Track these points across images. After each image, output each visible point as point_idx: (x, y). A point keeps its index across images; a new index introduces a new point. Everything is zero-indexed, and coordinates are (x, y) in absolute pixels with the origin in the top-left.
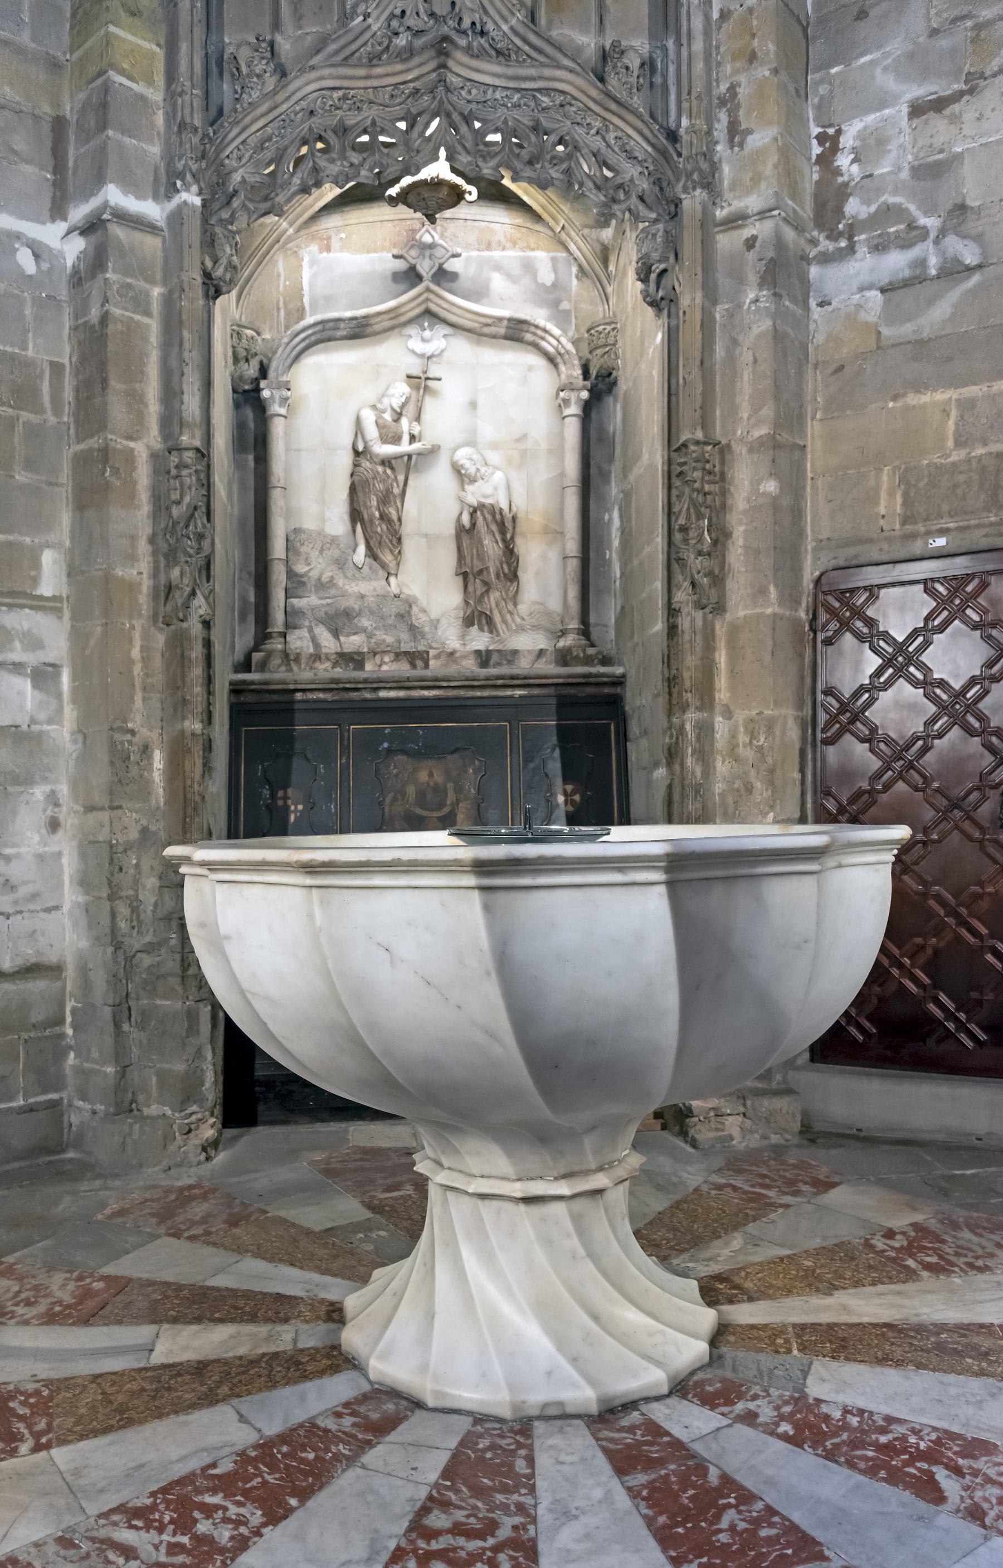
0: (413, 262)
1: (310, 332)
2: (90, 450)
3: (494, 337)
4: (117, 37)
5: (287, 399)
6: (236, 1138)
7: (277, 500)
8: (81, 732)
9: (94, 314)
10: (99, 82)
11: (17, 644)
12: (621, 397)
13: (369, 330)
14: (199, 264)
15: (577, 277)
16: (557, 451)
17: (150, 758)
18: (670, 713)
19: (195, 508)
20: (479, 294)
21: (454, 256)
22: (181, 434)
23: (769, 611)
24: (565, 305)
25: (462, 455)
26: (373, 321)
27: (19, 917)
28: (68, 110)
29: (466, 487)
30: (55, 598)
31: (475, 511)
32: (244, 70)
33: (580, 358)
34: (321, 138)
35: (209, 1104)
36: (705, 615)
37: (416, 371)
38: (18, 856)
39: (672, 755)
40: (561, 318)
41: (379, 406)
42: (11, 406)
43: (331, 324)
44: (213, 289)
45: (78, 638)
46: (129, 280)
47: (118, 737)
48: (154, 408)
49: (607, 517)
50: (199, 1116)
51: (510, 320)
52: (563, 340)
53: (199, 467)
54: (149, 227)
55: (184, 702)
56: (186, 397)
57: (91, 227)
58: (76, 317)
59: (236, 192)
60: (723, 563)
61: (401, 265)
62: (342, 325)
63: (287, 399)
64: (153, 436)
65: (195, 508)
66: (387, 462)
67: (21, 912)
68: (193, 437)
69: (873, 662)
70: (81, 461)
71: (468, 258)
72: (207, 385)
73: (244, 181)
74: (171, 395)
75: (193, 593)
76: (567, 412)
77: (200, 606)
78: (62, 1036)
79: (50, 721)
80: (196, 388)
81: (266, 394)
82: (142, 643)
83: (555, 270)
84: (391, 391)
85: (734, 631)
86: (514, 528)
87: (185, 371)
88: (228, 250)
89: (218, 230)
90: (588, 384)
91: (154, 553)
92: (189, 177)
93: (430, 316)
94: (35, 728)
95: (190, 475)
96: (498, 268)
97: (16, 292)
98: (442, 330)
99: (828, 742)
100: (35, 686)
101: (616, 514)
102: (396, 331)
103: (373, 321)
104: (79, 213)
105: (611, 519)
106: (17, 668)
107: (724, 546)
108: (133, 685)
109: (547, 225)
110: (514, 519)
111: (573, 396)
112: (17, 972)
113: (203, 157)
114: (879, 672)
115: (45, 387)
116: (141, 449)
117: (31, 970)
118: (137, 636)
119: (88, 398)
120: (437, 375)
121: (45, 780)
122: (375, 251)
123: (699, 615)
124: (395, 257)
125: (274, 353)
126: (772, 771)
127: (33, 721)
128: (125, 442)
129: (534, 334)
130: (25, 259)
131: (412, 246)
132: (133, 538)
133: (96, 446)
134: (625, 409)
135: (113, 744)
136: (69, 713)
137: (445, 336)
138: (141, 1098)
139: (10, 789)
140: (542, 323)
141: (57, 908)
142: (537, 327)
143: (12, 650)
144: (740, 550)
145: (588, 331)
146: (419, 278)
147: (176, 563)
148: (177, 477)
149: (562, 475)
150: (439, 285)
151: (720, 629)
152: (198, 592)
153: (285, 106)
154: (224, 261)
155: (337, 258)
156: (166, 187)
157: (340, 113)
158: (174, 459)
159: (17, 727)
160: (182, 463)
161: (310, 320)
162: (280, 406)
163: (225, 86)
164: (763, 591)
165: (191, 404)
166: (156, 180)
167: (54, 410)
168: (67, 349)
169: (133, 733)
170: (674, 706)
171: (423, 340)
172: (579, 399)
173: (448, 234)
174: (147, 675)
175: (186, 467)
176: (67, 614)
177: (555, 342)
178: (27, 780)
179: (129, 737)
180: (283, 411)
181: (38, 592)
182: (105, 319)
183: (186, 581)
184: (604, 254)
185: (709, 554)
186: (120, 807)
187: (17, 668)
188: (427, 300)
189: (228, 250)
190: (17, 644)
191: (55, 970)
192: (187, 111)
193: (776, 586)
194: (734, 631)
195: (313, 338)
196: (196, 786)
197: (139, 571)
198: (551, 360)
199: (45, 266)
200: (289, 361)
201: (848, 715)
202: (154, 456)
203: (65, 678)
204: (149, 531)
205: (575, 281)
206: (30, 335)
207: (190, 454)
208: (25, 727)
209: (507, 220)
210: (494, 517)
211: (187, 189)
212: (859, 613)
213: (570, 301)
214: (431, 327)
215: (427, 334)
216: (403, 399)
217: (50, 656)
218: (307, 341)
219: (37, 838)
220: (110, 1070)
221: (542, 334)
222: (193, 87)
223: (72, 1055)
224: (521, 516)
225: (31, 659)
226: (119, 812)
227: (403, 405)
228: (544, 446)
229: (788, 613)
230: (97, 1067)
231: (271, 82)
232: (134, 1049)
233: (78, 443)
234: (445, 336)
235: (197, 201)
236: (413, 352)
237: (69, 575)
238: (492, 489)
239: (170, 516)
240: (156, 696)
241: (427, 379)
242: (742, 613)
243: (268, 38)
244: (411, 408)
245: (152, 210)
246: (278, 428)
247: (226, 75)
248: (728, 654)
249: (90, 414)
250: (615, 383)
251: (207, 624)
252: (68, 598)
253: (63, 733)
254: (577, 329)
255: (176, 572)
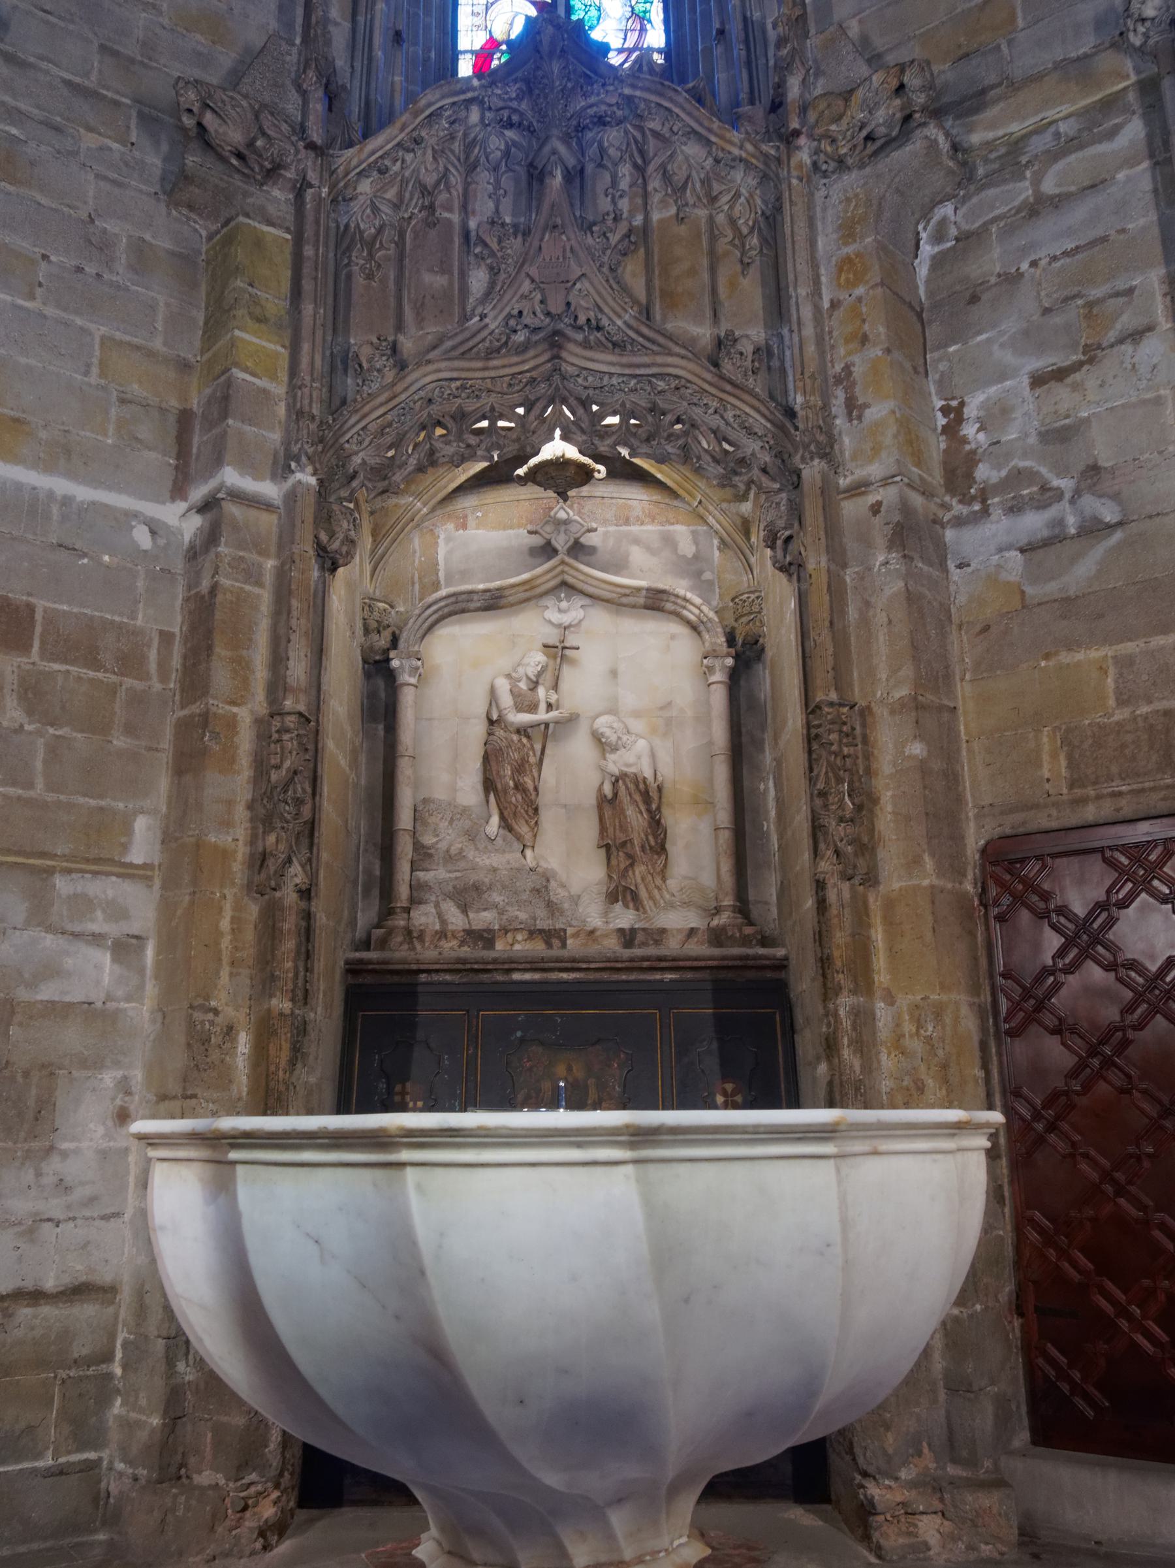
0: (548, 537)
1: (442, 604)
2: (192, 716)
3: (634, 606)
4: (242, 340)
5: (417, 668)
6: (311, 1521)
7: (405, 769)
8: (162, 1012)
9: (205, 585)
10: (223, 378)
11: (99, 914)
12: (768, 663)
13: (503, 601)
14: (312, 537)
15: (719, 549)
16: (703, 719)
17: (234, 1040)
18: (825, 998)
19: (295, 773)
20: (618, 565)
21: (590, 531)
22: (284, 699)
23: (926, 882)
24: (707, 576)
25: (603, 723)
26: (507, 593)
27: (71, 1224)
28: (195, 403)
29: (608, 755)
30: (145, 866)
31: (617, 781)
32: (365, 365)
33: (724, 627)
34: (439, 424)
35: (273, 1472)
36: (852, 886)
37: (553, 640)
38: (77, 1151)
39: (830, 1047)
40: (704, 588)
41: (514, 675)
42: (114, 673)
43: (464, 596)
44: (330, 563)
45: (166, 908)
46: (241, 554)
47: (198, 1015)
48: (260, 674)
49: (762, 787)
50: (259, 1488)
51: (648, 590)
52: (705, 608)
53: (302, 732)
54: (268, 507)
55: (273, 978)
56: (291, 664)
57: (207, 506)
58: (189, 590)
59: (355, 473)
60: (872, 830)
61: (537, 541)
62: (476, 597)
63: (417, 668)
64: (258, 702)
65: (295, 773)
66: (523, 731)
67: (74, 1219)
68: (297, 702)
69: (1053, 941)
70: (184, 728)
71: (606, 533)
72: (319, 651)
73: (364, 462)
74: (278, 661)
75: (289, 861)
76: (713, 679)
77: (297, 874)
78: (109, 1376)
79: (129, 999)
80: (302, 654)
81: (395, 663)
82: (232, 914)
83: (696, 543)
84: (525, 661)
85: (889, 905)
86: (660, 798)
87: (292, 637)
88: (345, 525)
89: (335, 507)
90: (732, 651)
91: (252, 820)
92: (304, 459)
93: (566, 587)
94: (111, 1005)
95: (292, 739)
96: (636, 541)
97: (129, 565)
98: (579, 601)
99: (1013, 1033)
100: (114, 960)
101: (771, 784)
102: (533, 602)
103: (507, 593)
104: (198, 493)
105: (766, 789)
106: (97, 939)
107: (871, 811)
108: (220, 960)
109: (683, 500)
110: (660, 789)
111: (717, 663)
112: (62, 1293)
113: (321, 441)
114: (1061, 953)
115: (153, 655)
116: (244, 715)
117: (79, 1291)
118: (228, 907)
119: (194, 665)
120: (575, 644)
121: (117, 1064)
122: (511, 528)
123: (846, 886)
124: (530, 532)
125: (406, 624)
126: (945, 1067)
127: (109, 998)
128: (227, 707)
129: (676, 603)
130: (142, 537)
131: (547, 523)
132: (230, 803)
133: (198, 711)
134: (772, 675)
135: (191, 1023)
136: (151, 989)
137: (582, 606)
138: (192, 1460)
139: (75, 1073)
140: (682, 592)
141: (116, 1215)
142: (677, 596)
143: (93, 920)
144: (889, 817)
145: (733, 600)
146: (555, 552)
147: (273, 829)
148: (278, 741)
149: (710, 743)
150: (576, 558)
151: (875, 903)
152: (294, 859)
153: (403, 397)
154: (341, 536)
155: (480, 536)
156: (281, 469)
157: (459, 401)
158: (276, 723)
159: (90, 1004)
160: (294, 731)
161: (443, 592)
162: (410, 676)
163: (349, 381)
164: (917, 861)
165: (297, 670)
166: (275, 462)
167: (159, 679)
168: (179, 619)
169: (216, 1012)
170: (828, 992)
171: (560, 611)
172: (724, 666)
173: (585, 510)
174: (236, 949)
175: (288, 731)
176: (157, 883)
177: (697, 611)
178: (95, 1064)
179: (210, 1016)
180: (413, 681)
181: (128, 859)
182: (214, 589)
183: (281, 847)
184: (745, 527)
185: (852, 821)
186: (194, 1096)
187: (97, 939)
188: (563, 572)
189: (345, 525)
190: (99, 914)
191: (103, 1292)
192: (306, 402)
193: (932, 855)
194: (889, 905)
195: (446, 610)
196: (281, 1073)
197: (234, 838)
198: (694, 628)
199: (161, 542)
200: (421, 631)
201: (1032, 1002)
202: (258, 721)
203: (150, 952)
204: (250, 797)
205: (717, 553)
206: (141, 605)
207: (293, 718)
208: (99, 1005)
209: (645, 497)
210: (637, 786)
211: (302, 470)
212: (1031, 886)
213: (713, 573)
214: (568, 598)
215: (564, 604)
216: (539, 668)
217: (135, 928)
218: (440, 613)
219: (101, 1130)
220: (156, 1421)
221: (684, 603)
222: (313, 380)
223: (119, 1401)
224: (667, 786)
225: (113, 930)
226: (194, 1101)
227: (539, 674)
228: (690, 713)
229: (949, 886)
230: (144, 1418)
231: (390, 375)
232: (189, 1396)
233: (182, 708)
234: (582, 606)
235: (313, 481)
236: (550, 622)
237: (163, 842)
238: (636, 756)
239: (269, 781)
240: (245, 972)
241: (564, 648)
242: (896, 885)
243: (391, 338)
244: (548, 677)
245: (269, 490)
246: (407, 698)
247: (350, 372)
248: (885, 931)
249: (194, 682)
250: (763, 650)
251: (306, 894)
252: (160, 865)
253: (141, 1013)
254: (721, 598)
255: (272, 838)
